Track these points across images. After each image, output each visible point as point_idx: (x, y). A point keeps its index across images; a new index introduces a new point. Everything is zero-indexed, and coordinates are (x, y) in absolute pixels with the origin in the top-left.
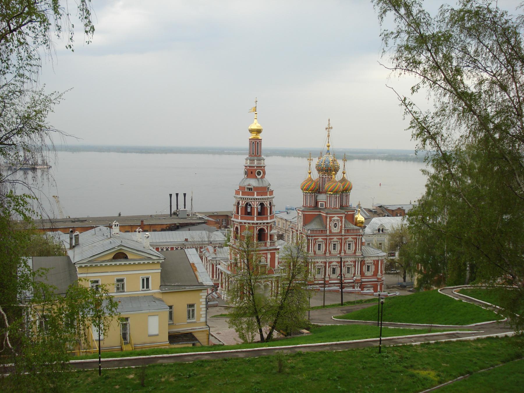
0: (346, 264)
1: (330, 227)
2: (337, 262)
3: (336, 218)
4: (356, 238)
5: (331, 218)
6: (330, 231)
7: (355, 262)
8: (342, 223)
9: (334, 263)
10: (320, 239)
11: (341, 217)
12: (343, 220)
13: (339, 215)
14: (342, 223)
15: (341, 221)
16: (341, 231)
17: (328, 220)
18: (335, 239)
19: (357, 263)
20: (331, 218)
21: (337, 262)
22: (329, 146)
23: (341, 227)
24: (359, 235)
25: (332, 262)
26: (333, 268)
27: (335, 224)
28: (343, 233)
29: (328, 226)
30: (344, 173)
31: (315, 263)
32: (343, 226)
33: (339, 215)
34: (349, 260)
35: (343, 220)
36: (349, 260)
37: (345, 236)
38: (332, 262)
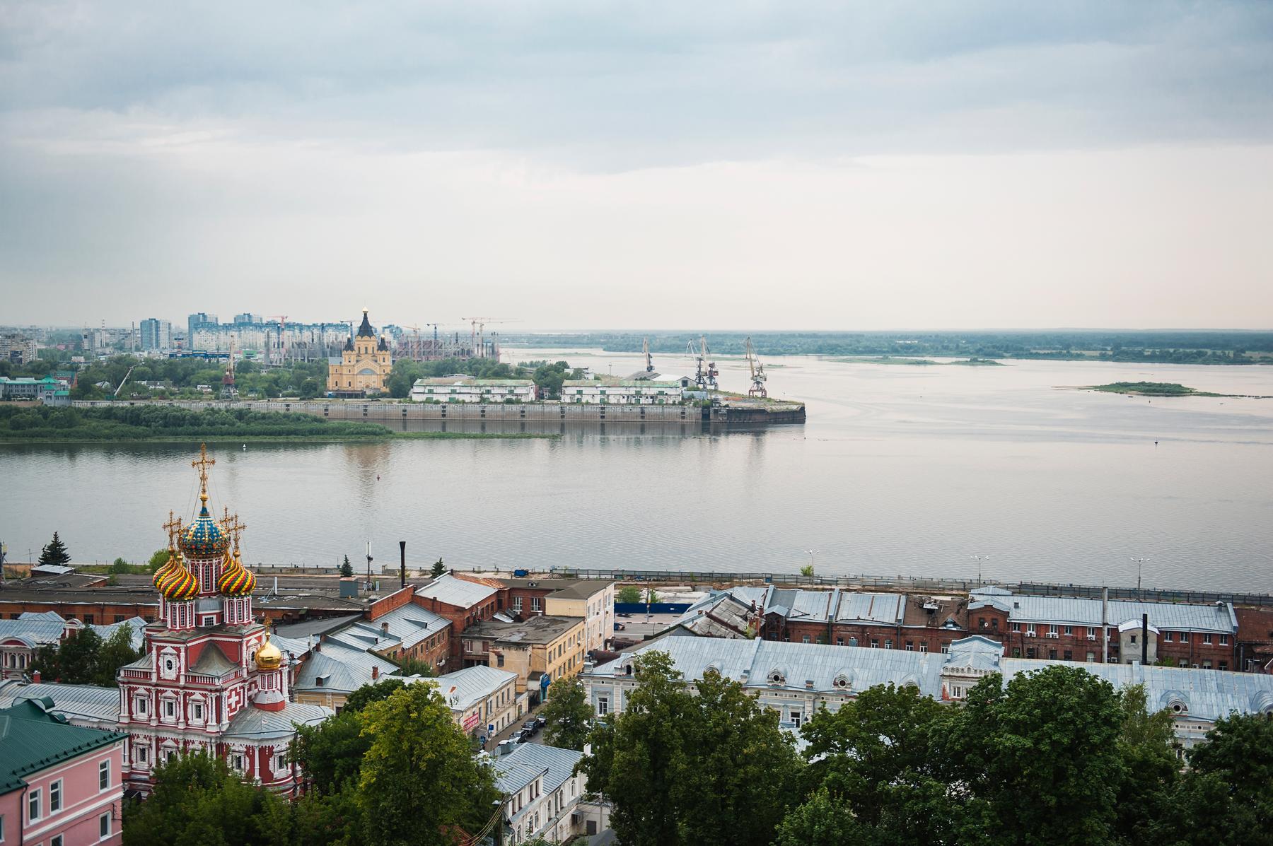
1: (158, 667)
2: (176, 741)
5: (159, 649)
6: (159, 678)
10: (141, 690)
11: (178, 649)
12: (183, 654)
15: (179, 656)
17: (154, 652)
18: (169, 693)
20: (159, 649)
22: (204, 500)
25: (164, 740)
27: (169, 662)
28: (182, 683)
35: (183, 654)
36: (197, 739)
37: (184, 688)
38: (164, 740)
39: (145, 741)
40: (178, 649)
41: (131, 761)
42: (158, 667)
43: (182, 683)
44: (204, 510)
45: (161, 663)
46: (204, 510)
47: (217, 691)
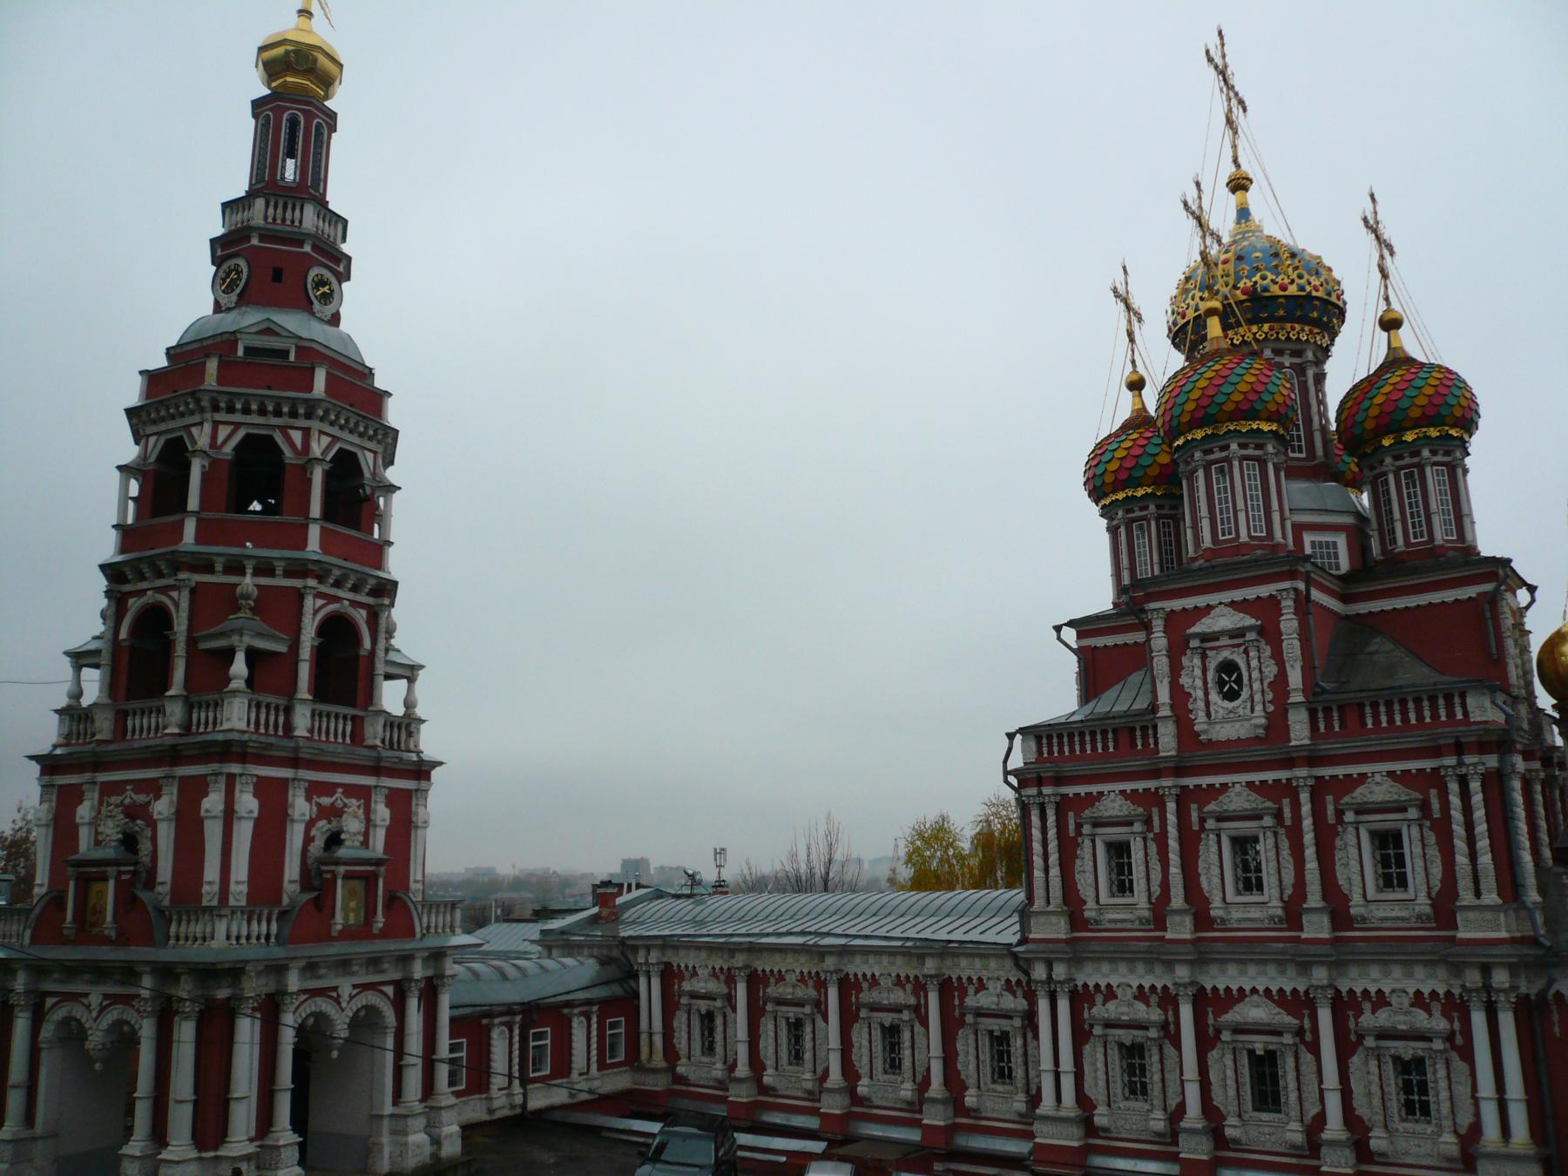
0: (1370, 1020)
1: (1180, 696)
2: (1283, 1000)
3: (1224, 620)
4: (1435, 779)
5: (1177, 624)
7: (1456, 1007)
8: (1278, 656)
9: (1256, 1012)
10: (1113, 804)
11: (1267, 610)
12: (1289, 624)
13: (1250, 593)
14: (1278, 656)
15: (1270, 634)
16: (1277, 724)
18: (1238, 792)
19: (1478, 1020)
21: (1283, 1000)
23: (1280, 684)
24: (1459, 749)
26: (1251, 1053)
27: (1228, 667)
29: (1164, 695)
30: (1390, 324)
31: (1081, 998)
32: (1295, 678)
33: (1250, 593)
34: (1399, 990)
35: (1289, 624)
36: (1397, 982)
37: (1313, 760)
39: (1141, 1011)
40: (1267, 610)
41: (1082, 1099)
42: (1180, 696)
43: (1299, 731)
44: (1243, 213)
45: (1191, 679)
46: (1243, 213)
47: (1482, 748)
